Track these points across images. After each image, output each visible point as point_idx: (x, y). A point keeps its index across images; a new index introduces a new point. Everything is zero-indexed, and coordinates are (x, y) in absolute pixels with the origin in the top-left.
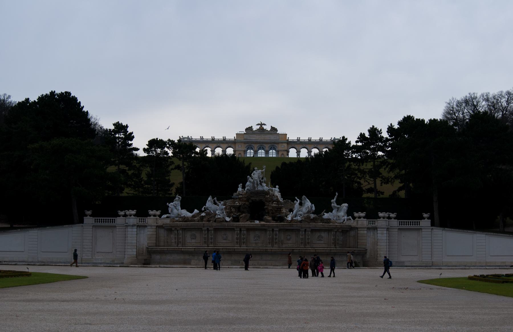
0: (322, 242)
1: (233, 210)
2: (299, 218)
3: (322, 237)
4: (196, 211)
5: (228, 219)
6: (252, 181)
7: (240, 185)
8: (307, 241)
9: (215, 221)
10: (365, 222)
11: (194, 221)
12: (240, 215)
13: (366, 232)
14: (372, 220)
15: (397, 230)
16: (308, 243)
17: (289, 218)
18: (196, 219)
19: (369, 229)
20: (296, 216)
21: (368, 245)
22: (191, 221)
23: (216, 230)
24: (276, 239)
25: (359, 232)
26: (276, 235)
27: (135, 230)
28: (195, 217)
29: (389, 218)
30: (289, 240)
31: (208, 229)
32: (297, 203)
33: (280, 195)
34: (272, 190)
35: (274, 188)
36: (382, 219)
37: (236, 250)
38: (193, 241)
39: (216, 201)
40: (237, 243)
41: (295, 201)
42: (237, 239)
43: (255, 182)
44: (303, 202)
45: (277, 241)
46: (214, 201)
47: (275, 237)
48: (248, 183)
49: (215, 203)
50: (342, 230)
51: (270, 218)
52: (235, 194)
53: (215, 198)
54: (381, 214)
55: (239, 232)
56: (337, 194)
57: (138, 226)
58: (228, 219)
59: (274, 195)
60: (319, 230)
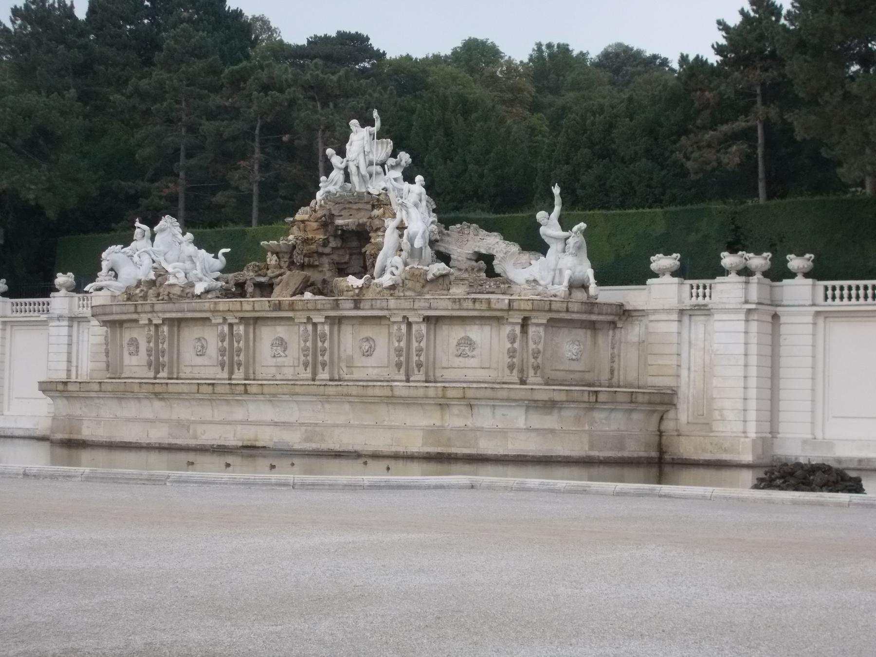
0: (472, 362)
2: (386, 280)
8: (415, 358)
10: (675, 288)
12: (277, 276)
13: (674, 327)
14: (701, 282)
15: (810, 319)
16: (419, 365)
19: (681, 312)
21: (684, 373)
23: (177, 323)
24: (324, 351)
25: (653, 327)
26: (323, 337)
27: (65, 331)
29: (778, 272)
30: (368, 354)
31: (150, 320)
35: (406, 185)
36: (733, 277)
37: (171, 389)
42: (222, 352)
50: (551, 320)
54: (728, 260)
56: (556, 190)
57: (72, 319)
60: (463, 320)
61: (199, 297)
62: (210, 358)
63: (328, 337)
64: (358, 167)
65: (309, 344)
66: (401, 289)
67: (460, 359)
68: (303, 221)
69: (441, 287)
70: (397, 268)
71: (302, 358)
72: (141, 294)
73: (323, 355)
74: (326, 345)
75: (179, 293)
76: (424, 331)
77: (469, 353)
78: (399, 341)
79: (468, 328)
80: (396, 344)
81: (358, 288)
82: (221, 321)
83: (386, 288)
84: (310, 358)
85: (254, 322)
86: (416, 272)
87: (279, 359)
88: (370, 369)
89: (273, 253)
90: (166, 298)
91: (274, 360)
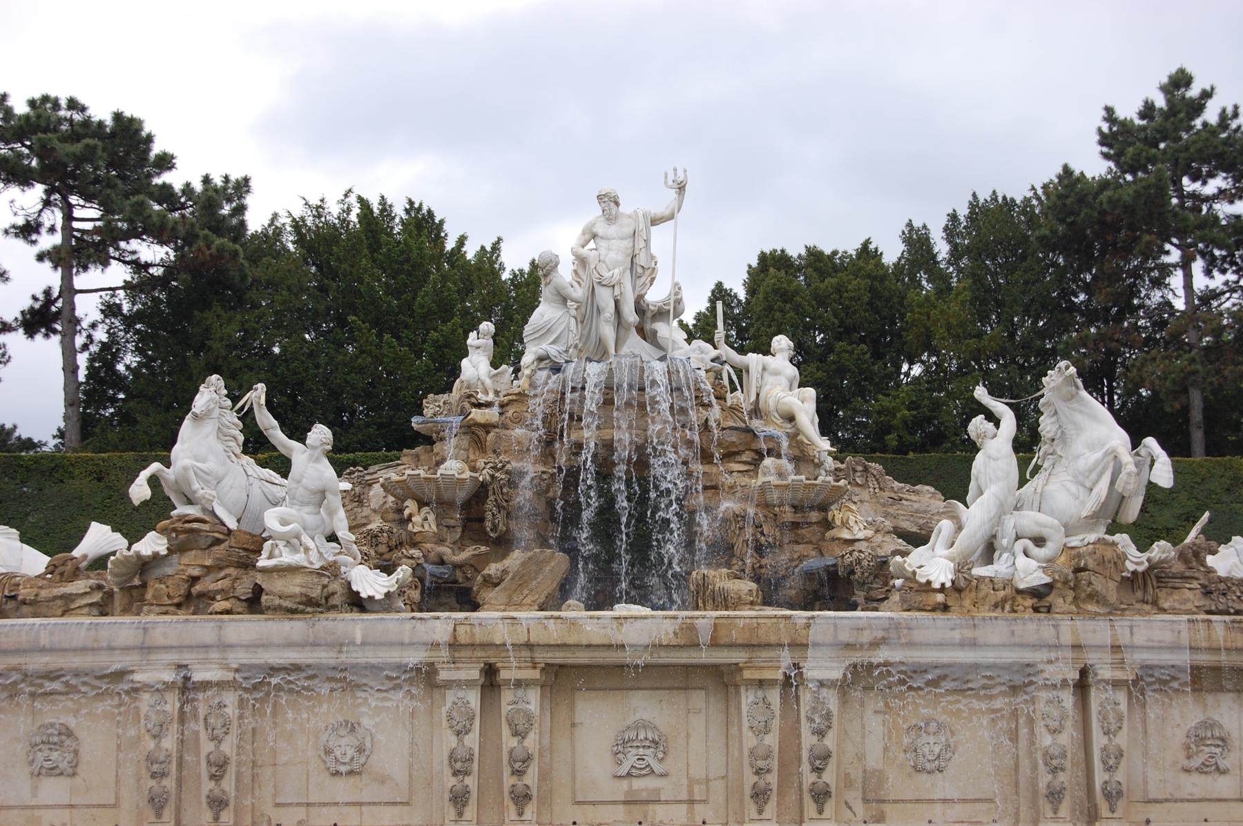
0: (1224, 786)
1: (423, 521)
2: (1028, 571)
3: (1224, 741)
4: (99, 538)
5: (370, 583)
6: (579, 293)
7: (480, 341)
8: (1100, 777)
9: (254, 603)
11: (66, 605)
16: (1113, 796)
17: (934, 565)
18: (80, 586)
20: (989, 551)
22: (35, 607)
24: (820, 761)
28: (76, 574)
32: (995, 444)
33: (812, 406)
34: (741, 372)
35: (753, 359)
38: (54, 790)
39: (267, 422)
40: (459, 799)
41: (978, 424)
43: (605, 299)
44: (1047, 426)
45: (829, 777)
46: (247, 418)
47: (808, 739)
48: (544, 313)
49: (256, 444)
51: (746, 586)
52: (432, 404)
53: (258, 394)
55: (473, 698)
58: (370, 583)
59: (756, 412)
61: (357, 603)
62: (383, 780)
63: (835, 720)
64: (617, 302)
65: (772, 740)
66: (1071, 594)
67: (1195, 777)
68: (487, 427)
69: (1139, 594)
70: (1039, 541)
71: (750, 779)
72: (97, 597)
73: (818, 770)
74: (830, 741)
75: (316, 593)
76: (1123, 707)
77: (1223, 764)
78: (1054, 732)
79: (1210, 699)
80: (1047, 740)
81: (943, 588)
82: (475, 674)
83: (1019, 592)
84: (773, 779)
85: (566, 676)
86: (1109, 554)
87: (637, 784)
88: (938, 807)
89: (422, 504)
90: (239, 607)
91: (624, 784)
